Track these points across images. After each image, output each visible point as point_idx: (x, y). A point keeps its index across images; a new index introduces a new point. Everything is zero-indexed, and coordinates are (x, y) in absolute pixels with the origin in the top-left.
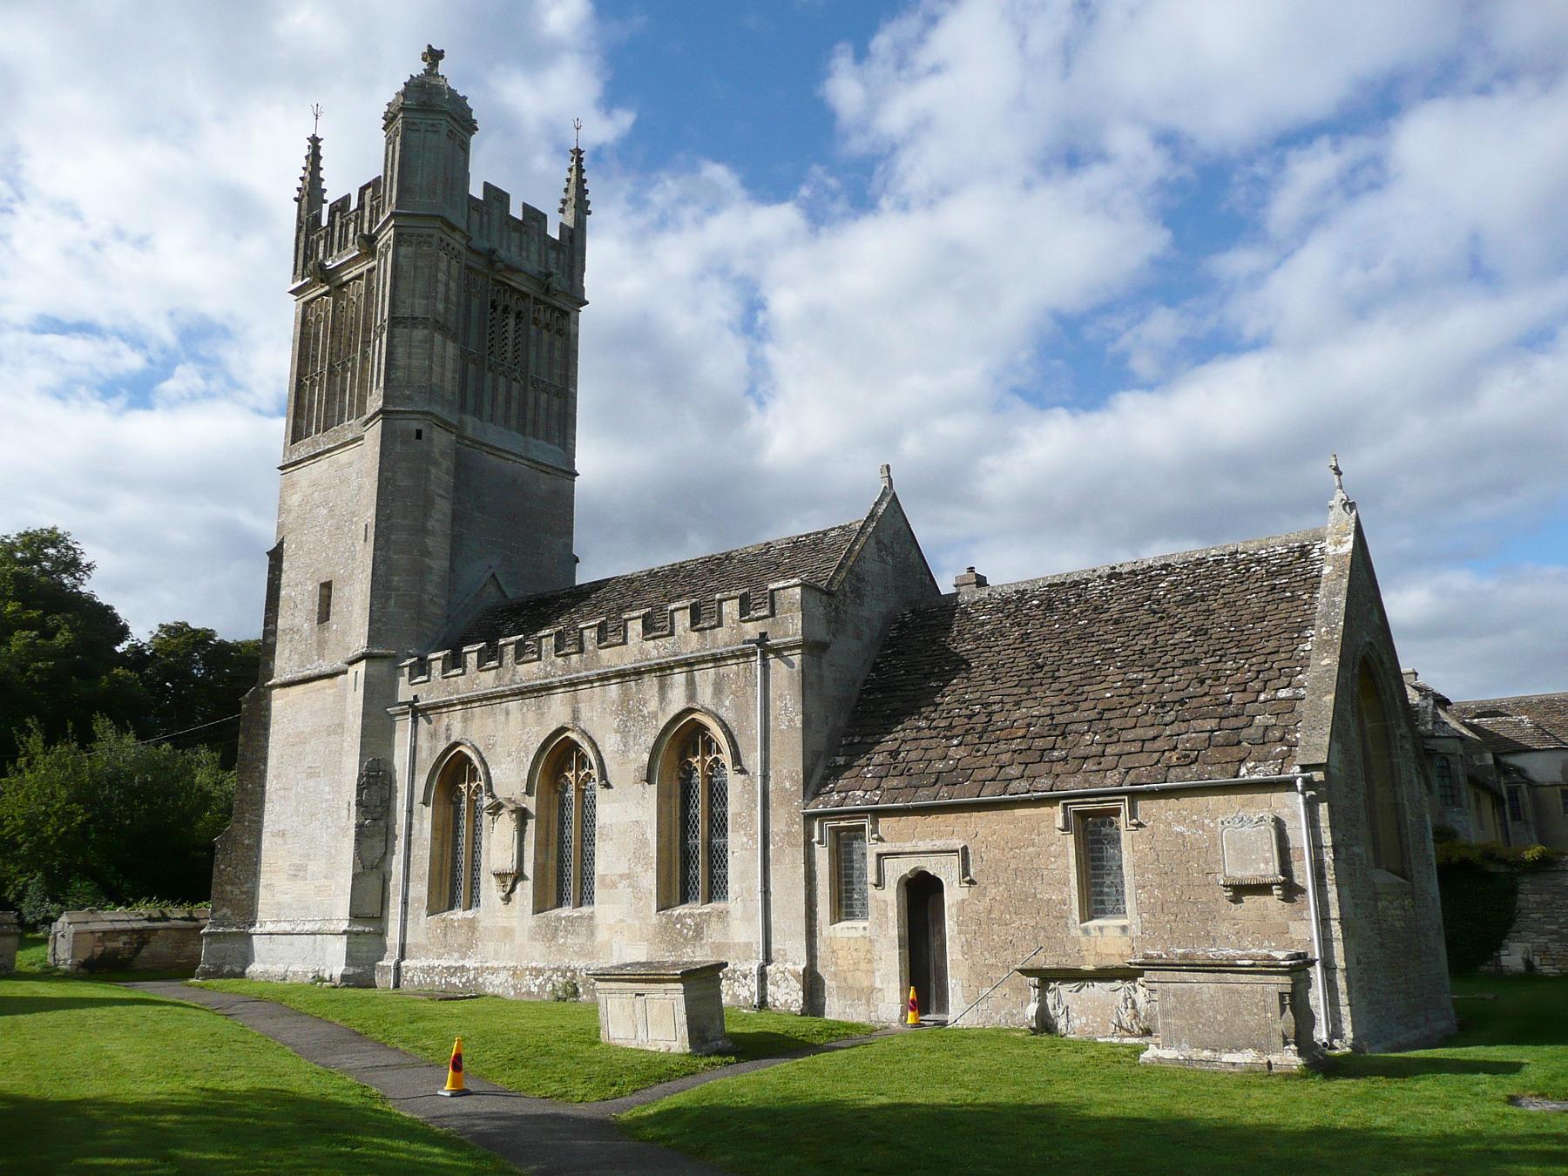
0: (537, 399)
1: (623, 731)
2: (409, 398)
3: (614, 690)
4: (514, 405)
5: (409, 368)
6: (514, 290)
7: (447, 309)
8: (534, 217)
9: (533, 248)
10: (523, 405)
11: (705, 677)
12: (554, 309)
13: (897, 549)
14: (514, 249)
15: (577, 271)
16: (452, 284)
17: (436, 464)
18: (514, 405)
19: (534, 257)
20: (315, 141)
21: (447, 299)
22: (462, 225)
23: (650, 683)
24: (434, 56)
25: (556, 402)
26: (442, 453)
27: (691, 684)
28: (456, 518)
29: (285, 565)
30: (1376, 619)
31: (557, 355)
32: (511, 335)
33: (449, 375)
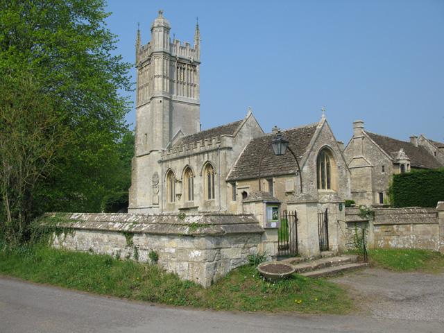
3: (196, 157)
11: (210, 154)
20: (139, 31)
23: (201, 155)
30: (332, 139)
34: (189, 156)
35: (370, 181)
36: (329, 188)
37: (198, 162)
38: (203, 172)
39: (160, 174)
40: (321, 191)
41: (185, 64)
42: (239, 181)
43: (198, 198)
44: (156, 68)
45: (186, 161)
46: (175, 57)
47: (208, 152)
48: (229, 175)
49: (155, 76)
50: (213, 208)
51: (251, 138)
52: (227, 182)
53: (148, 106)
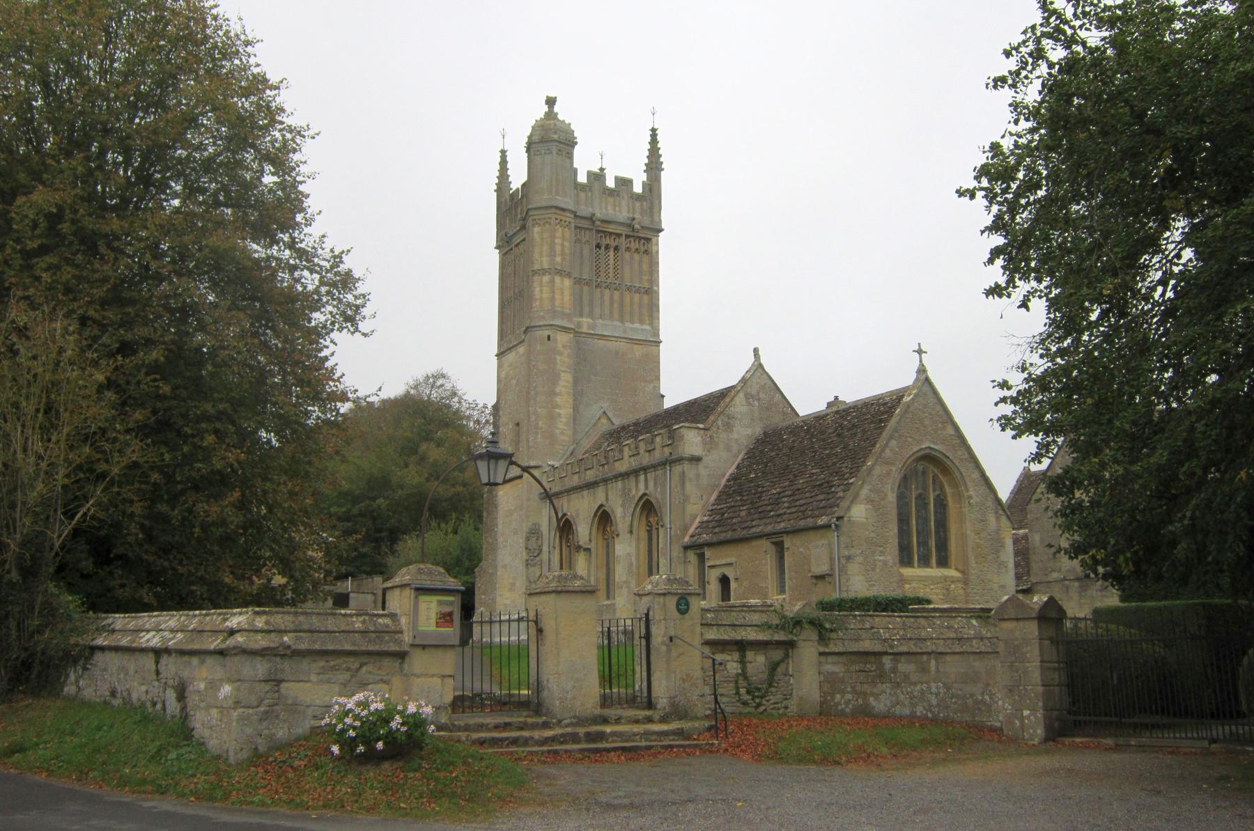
0: (632, 299)
1: (623, 505)
2: (543, 317)
4: (616, 306)
5: (541, 299)
6: (611, 234)
7: (563, 259)
8: (624, 183)
9: (624, 203)
10: (622, 305)
12: (640, 238)
13: (762, 395)
14: (609, 207)
15: (656, 210)
16: (566, 244)
17: (560, 354)
18: (616, 306)
19: (625, 209)
21: (563, 254)
22: (571, 207)
23: (632, 479)
24: (551, 102)
25: (646, 298)
26: (564, 346)
28: (576, 381)
30: (950, 431)
31: (645, 267)
32: (611, 262)
33: (567, 298)
34: (605, 481)
36: (943, 562)
37: (625, 494)
38: (635, 524)
39: (544, 528)
40: (907, 572)
41: (619, 235)
42: (710, 545)
44: (537, 250)
45: (599, 496)
46: (591, 219)
47: (645, 469)
48: (692, 530)
49: (535, 272)
51: (758, 431)
52: (686, 548)
53: (521, 349)
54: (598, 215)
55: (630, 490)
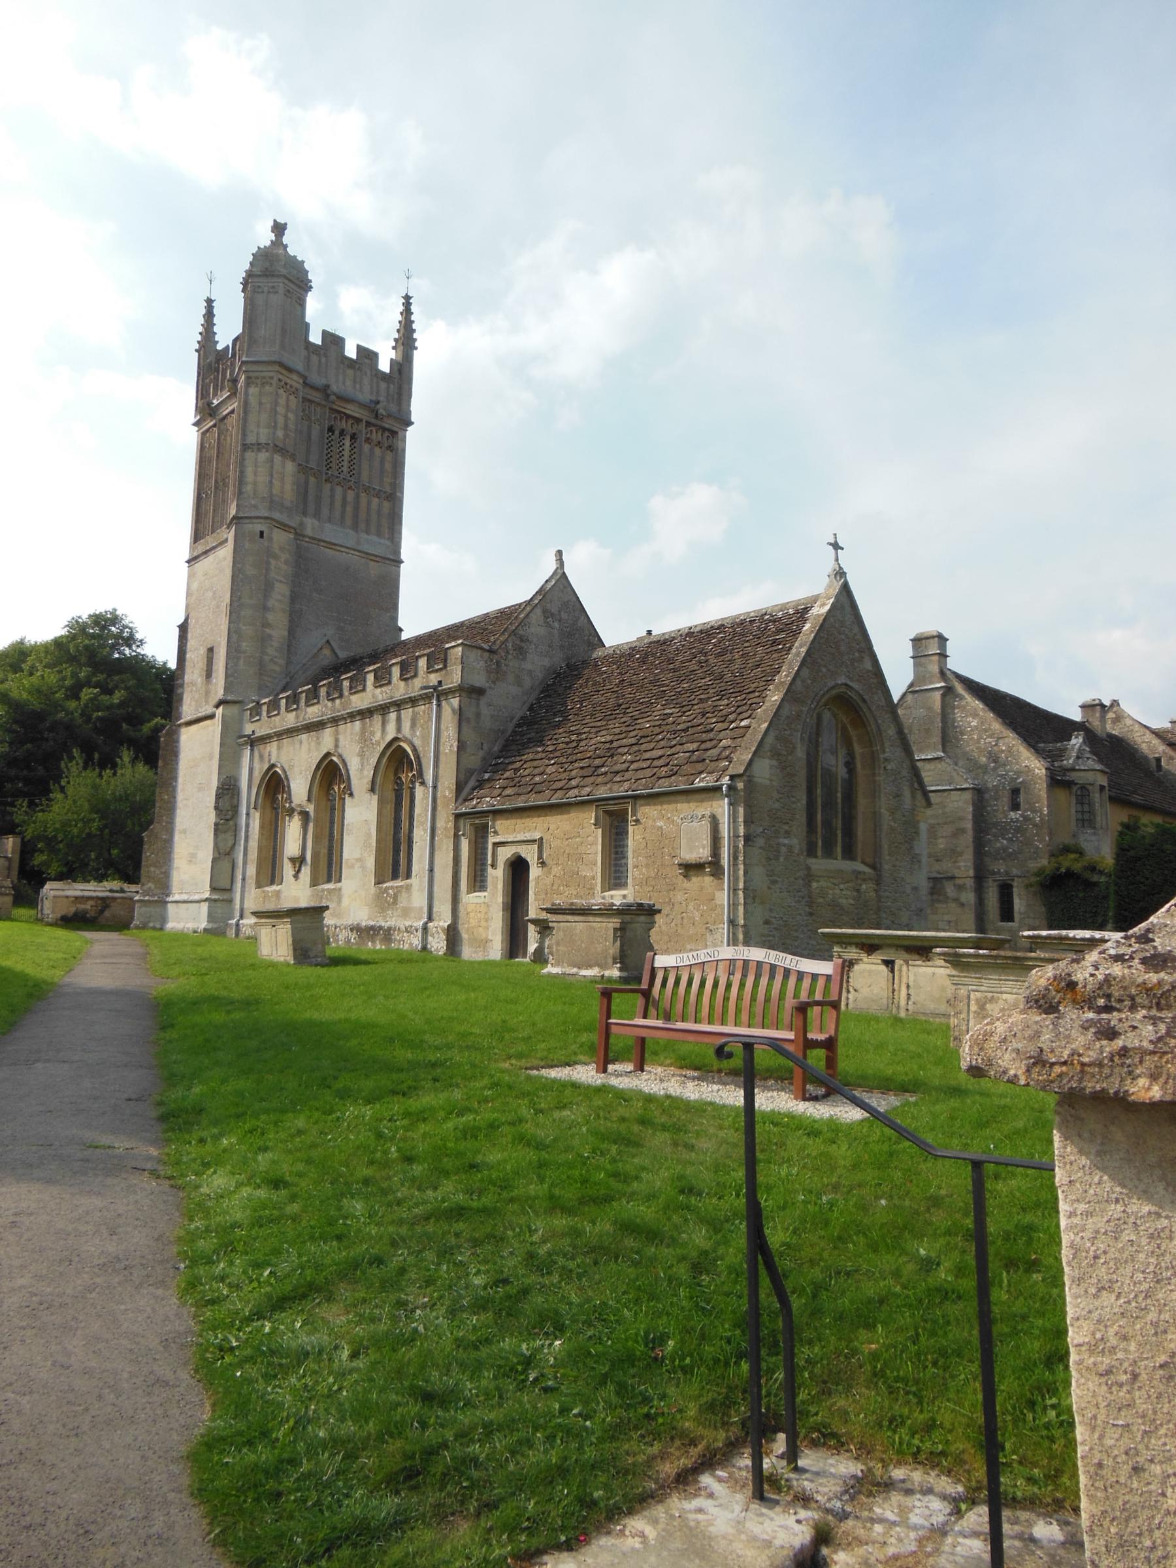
0: (369, 503)
1: (361, 755)
2: (255, 506)
4: (349, 509)
5: (255, 483)
6: (348, 416)
7: (286, 436)
8: (367, 356)
9: (366, 381)
11: (407, 714)
12: (384, 429)
13: (564, 616)
16: (291, 415)
17: (276, 557)
18: (349, 509)
19: (367, 388)
20: (210, 302)
21: (286, 427)
22: (300, 367)
23: (377, 718)
26: (281, 549)
27: (399, 719)
28: (294, 598)
29: (189, 636)
31: (388, 466)
32: (346, 453)
33: (288, 487)
34: (335, 721)
35: (968, 838)
36: (849, 853)
41: (358, 421)
43: (357, 870)
46: (325, 390)
47: (398, 705)
50: (406, 913)
54: (334, 388)
55: (373, 733)
